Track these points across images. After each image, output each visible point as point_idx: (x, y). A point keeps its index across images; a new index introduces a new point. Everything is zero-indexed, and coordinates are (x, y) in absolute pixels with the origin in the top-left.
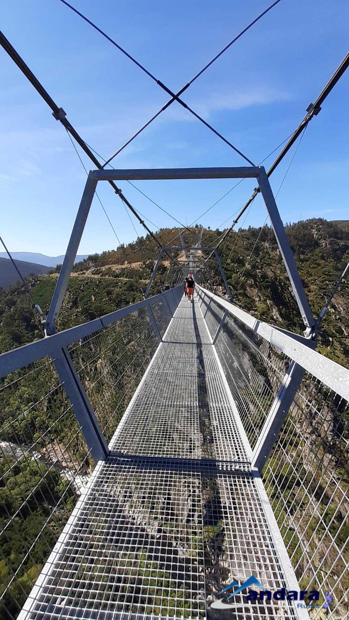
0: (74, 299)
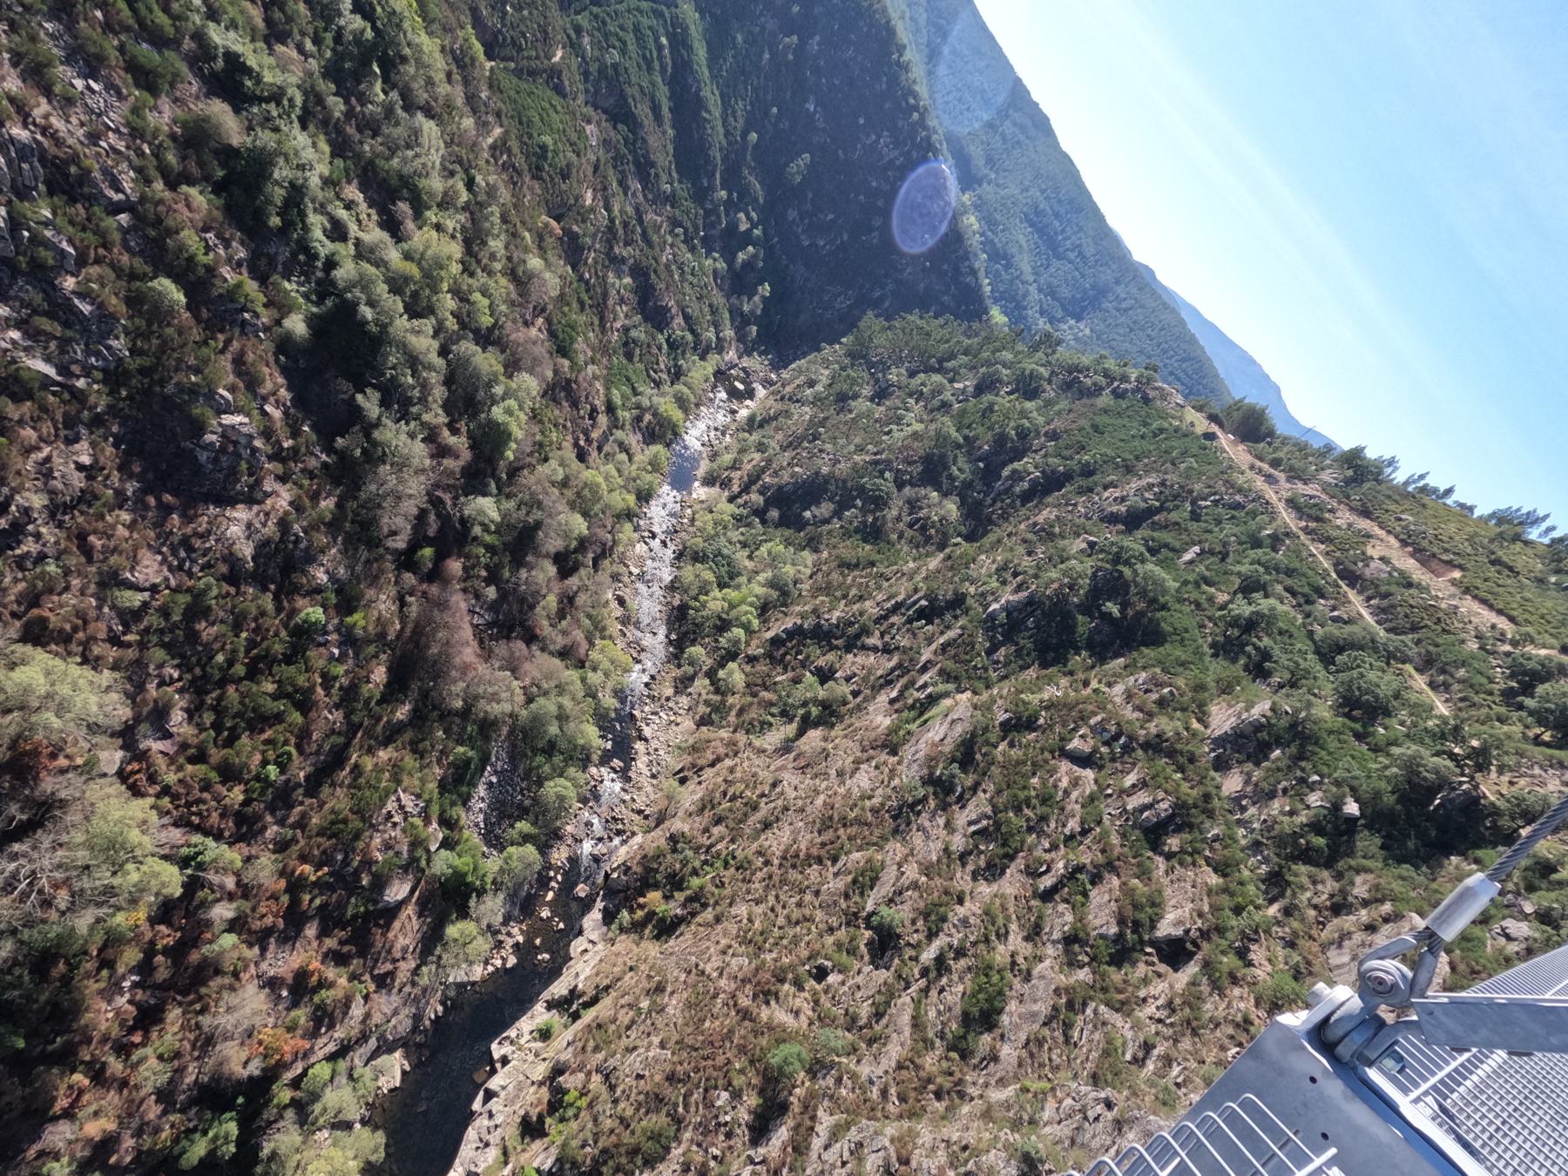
0: (1143, 505)
